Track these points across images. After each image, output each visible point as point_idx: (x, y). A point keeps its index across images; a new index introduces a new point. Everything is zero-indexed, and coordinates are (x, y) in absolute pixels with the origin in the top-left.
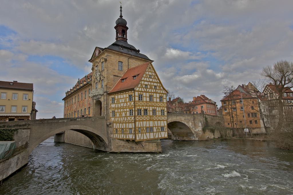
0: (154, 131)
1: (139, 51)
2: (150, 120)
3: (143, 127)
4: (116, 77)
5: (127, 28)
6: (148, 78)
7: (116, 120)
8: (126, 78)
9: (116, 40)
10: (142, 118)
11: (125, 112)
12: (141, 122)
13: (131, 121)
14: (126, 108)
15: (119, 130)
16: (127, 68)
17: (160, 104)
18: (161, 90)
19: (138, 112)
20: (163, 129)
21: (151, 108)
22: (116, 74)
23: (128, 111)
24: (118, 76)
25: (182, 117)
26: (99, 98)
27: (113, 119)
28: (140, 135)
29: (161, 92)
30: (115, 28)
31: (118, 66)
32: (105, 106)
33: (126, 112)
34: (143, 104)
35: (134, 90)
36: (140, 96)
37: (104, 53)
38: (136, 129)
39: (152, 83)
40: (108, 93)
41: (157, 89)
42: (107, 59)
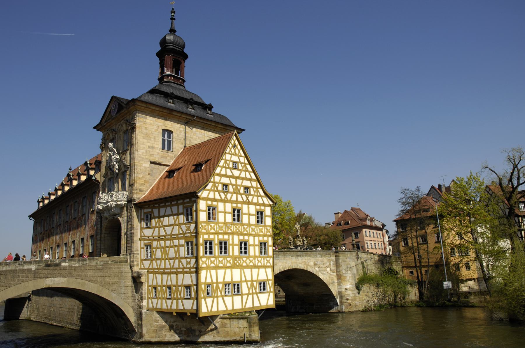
0: (244, 293)
2: (234, 266)
3: (217, 283)
4: (157, 166)
5: (186, 57)
7: (155, 266)
9: (158, 82)
10: (215, 262)
12: (213, 272)
13: (190, 268)
14: (179, 239)
18: (260, 196)
19: (206, 248)
21: (236, 237)
22: (157, 160)
23: (182, 246)
24: (160, 164)
27: (147, 263)
28: (209, 301)
29: (260, 202)
30: (158, 54)
34: (217, 228)
35: (198, 197)
39: (238, 180)
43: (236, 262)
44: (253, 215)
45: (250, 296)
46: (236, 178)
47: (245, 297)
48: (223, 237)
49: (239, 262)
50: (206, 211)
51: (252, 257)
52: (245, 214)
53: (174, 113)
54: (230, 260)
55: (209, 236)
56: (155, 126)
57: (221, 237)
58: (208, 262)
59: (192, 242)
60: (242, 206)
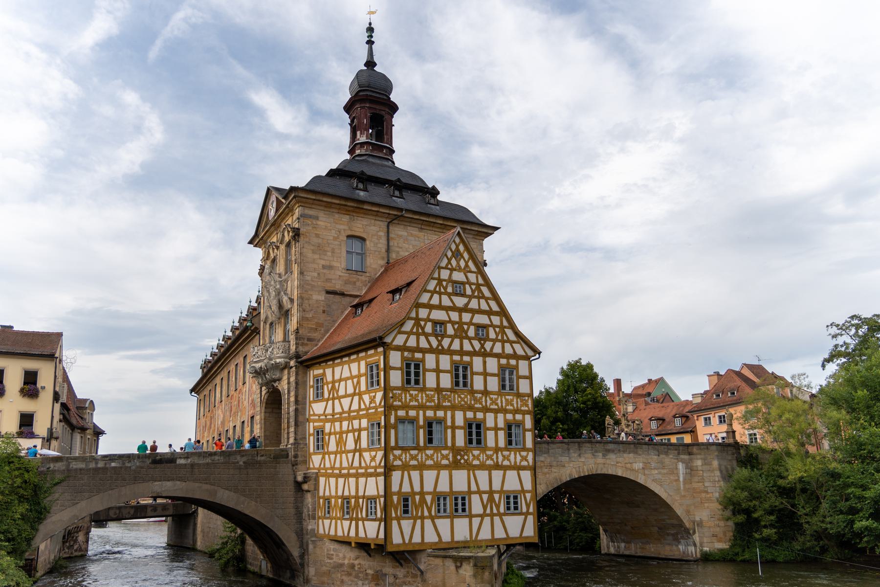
0: (474, 512)
1: (434, 192)
2: (456, 465)
3: (422, 493)
6: (446, 293)
7: (328, 465)
8: (371, 301)
10: (419, 457)
11: (356, 434)
13: (375, 468)
14: (359, 417)
15: (336, 502)
16: (383, 262)
17: (501, 401)
18: (508, 341)
20: (516, 503)
22: (338, 286)
23: (365, 429)
25: (631, 455)
26: (275, 381)
28: (406, 524)
31: (344, 254)
32: (292, 409)
33: (360, 430)
34: (422, 398)
36: (412, 369)
37: (293, 207)
38: (392, 501)
39: (464, 314)
40: (304, 358)
41: (487, 339)
42: (302, 230)
43: (459, 457)
44: (493, 375)
45: (487, 520)
46: (461, 310)
47: (476, 521)
48: (435, 414)
49: (466, 457)
50: (400, 369)
51: (490, 449)
52: (477, 374)
53: (366, 207)
54: (448, 455)
55: (407, 413)
56: (333, 231)
57: (430, 413)
58: (405, 457)
59: (379, 424)
60: (472, 360)
